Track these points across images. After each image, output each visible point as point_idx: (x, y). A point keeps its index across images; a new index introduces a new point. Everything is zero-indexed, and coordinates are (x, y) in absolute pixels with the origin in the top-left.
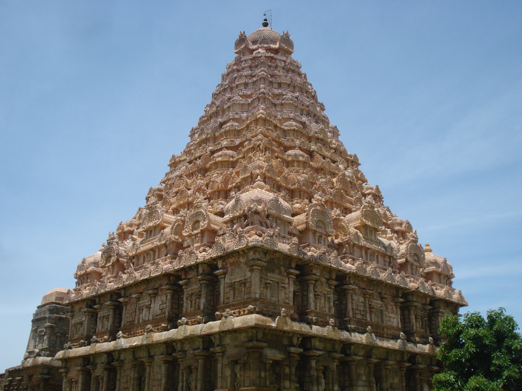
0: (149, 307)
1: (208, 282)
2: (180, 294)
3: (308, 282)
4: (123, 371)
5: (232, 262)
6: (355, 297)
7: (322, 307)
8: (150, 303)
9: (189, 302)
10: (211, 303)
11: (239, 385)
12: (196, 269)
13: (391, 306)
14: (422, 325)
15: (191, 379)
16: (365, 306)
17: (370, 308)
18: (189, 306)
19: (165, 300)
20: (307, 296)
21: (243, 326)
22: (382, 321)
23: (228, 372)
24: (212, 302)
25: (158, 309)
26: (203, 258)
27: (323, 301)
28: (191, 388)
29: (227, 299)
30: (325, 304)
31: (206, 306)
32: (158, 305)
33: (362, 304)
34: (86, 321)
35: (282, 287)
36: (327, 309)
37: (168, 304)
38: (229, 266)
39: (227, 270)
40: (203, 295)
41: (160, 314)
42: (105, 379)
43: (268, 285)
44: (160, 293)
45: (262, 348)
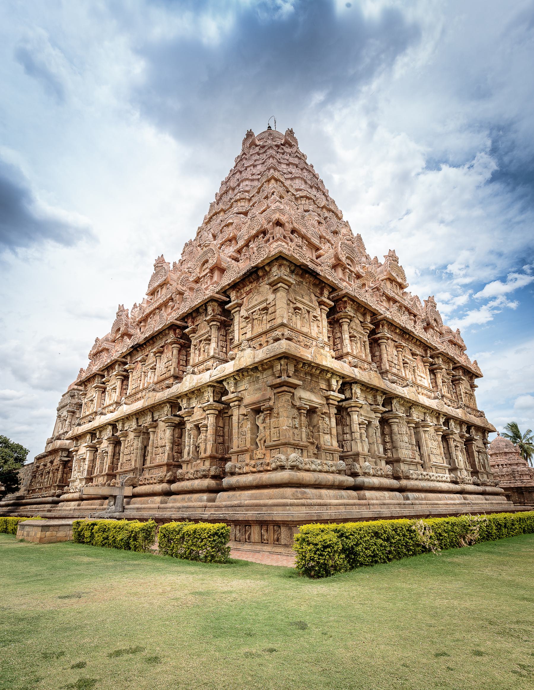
0: (154, 368)
1: (219, 324)
2: (188, 350)
4: (127, 442)
5: (248, 289)
6: (389, 349)
8: (155, 363)
9: (197, 352)
10: (223, 349)
11: (262, 442)
12: (205, 313)
13: (421, 365)
14: (448, 390)
15: (199, 441)
16: (398, 360)
17: (404, 364)
18: (197, 355)
19: (171, 356)
20: (341, 338)
22: (415, 378)
24: (224, 349)
25: (163, 367)
26: (212, 291)
27: (359, 345)
29: (242, 335)
30: (361, 349)
31: (217, 351)
32: (164, 364)
33: (396, 358)
34: (96, 396)
35: (315, 317)
36: (364, 355)
37: (175, 360)
38: (244, 295)
39: (243, 302)
40: (214, 339)
41: (165, 373)
42: (110, 454)
43: (297, 310)
44: (166, 351)
45: (295, 387)
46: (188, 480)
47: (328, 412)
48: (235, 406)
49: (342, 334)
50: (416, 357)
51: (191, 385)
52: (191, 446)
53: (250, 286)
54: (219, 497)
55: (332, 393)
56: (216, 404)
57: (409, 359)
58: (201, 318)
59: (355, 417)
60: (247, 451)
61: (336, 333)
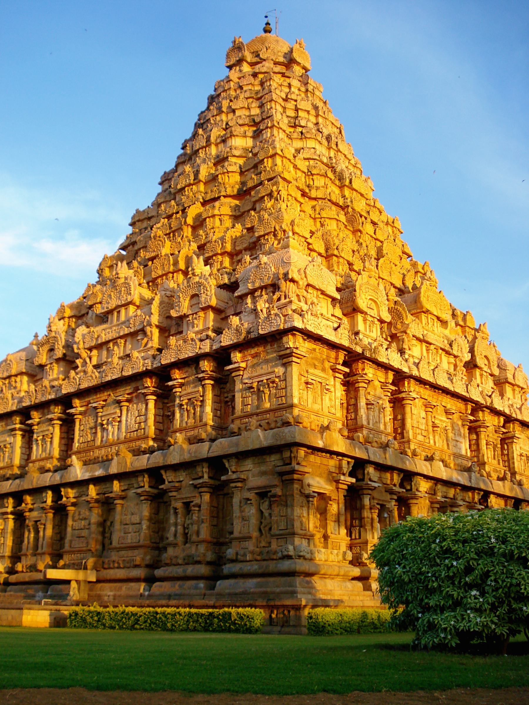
2: (166, 401)
3: (357, 385)
6: (415, 411)
7: (376, 422)
11: (267, 528)
14: (494, 455)
16: (427, 425)
21: (279, 443)
23: (252, 511)
24: (219, 412)
28: (189, 535)
35: (327, 390)
46: (175, 565)
47: (337, 498)
48: (236, 487)
49: (357, 400)
50: (450, 417)
51: (182, 458)
52: (179, 527)
53: (256, 349)
54: (220, 585)
55: (342, 478)
56: (212, 482)
57: (441, 420)
58: (190, 370)
59: (367, 501)
60: (250, 538)
61: (351, 398)
